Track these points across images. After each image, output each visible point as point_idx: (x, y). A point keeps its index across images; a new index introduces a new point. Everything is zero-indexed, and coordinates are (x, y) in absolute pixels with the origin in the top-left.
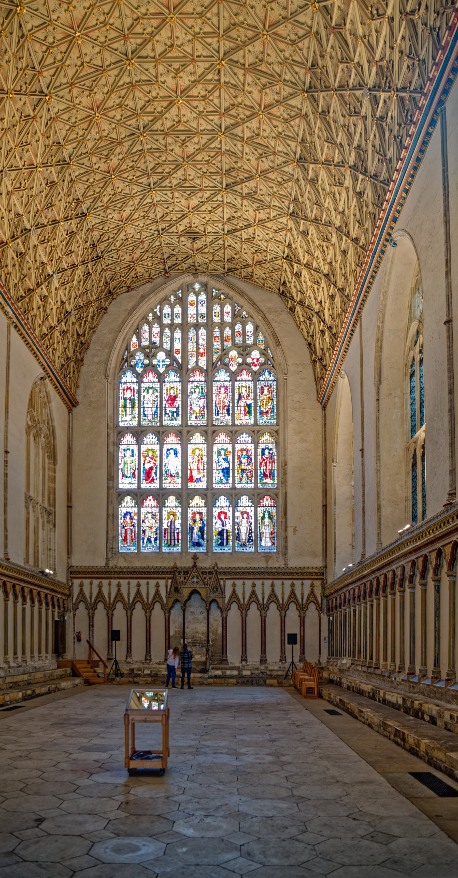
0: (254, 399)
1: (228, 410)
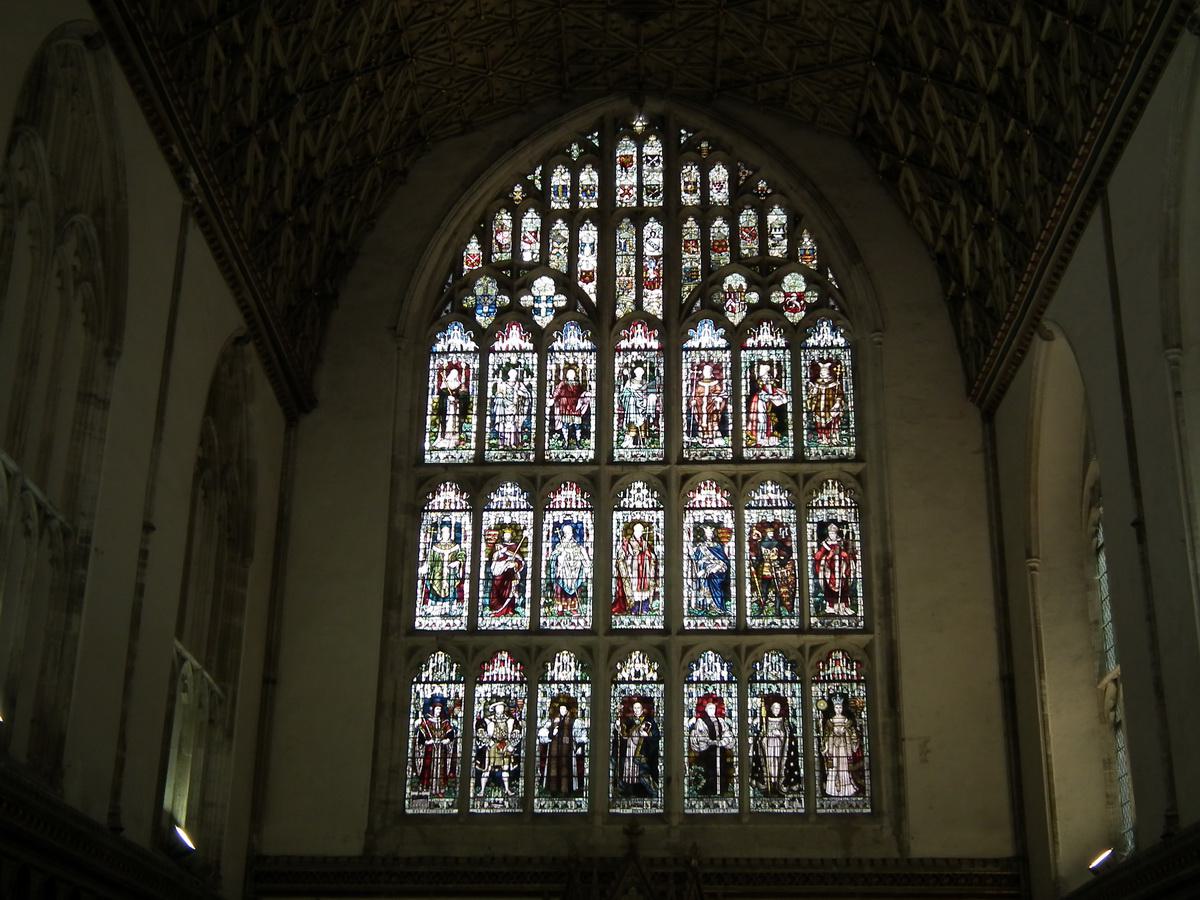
0: (792, 394)
1: (723, 423)
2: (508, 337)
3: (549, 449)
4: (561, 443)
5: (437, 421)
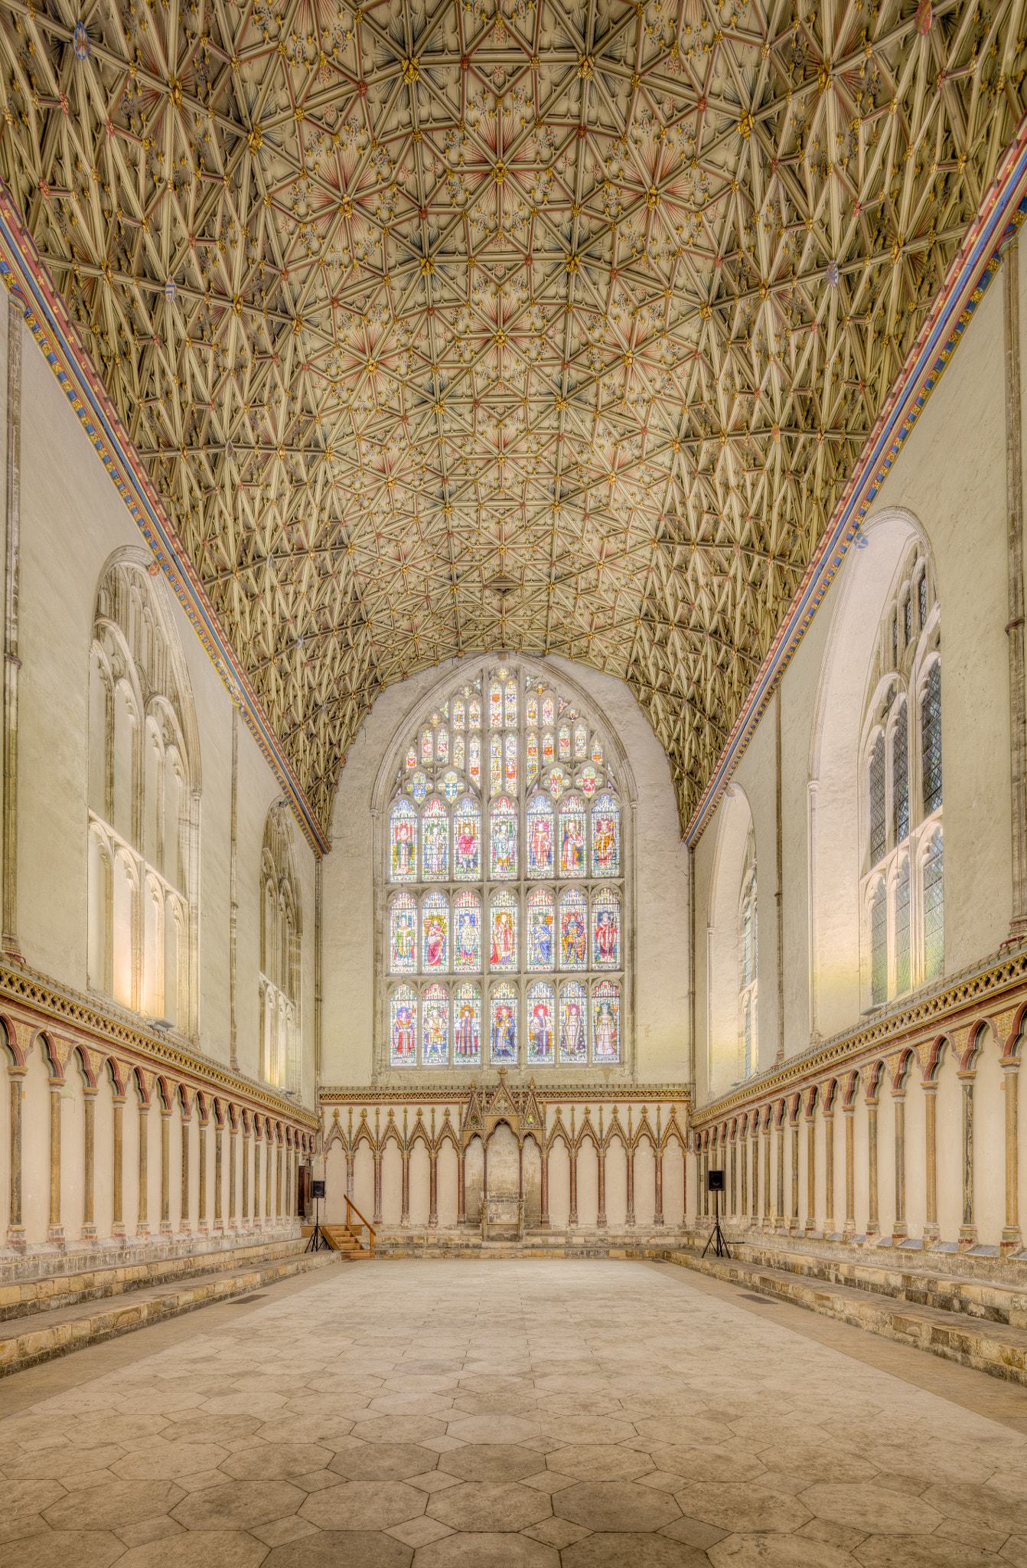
1: (549, 856)
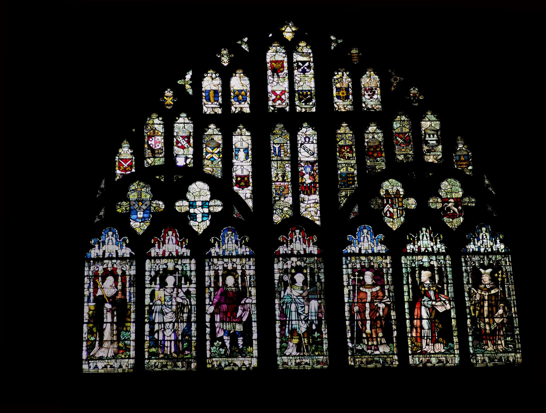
2: (164, 243)
3: (211, 357)
4: (222, 351)
5: (94, 330)
